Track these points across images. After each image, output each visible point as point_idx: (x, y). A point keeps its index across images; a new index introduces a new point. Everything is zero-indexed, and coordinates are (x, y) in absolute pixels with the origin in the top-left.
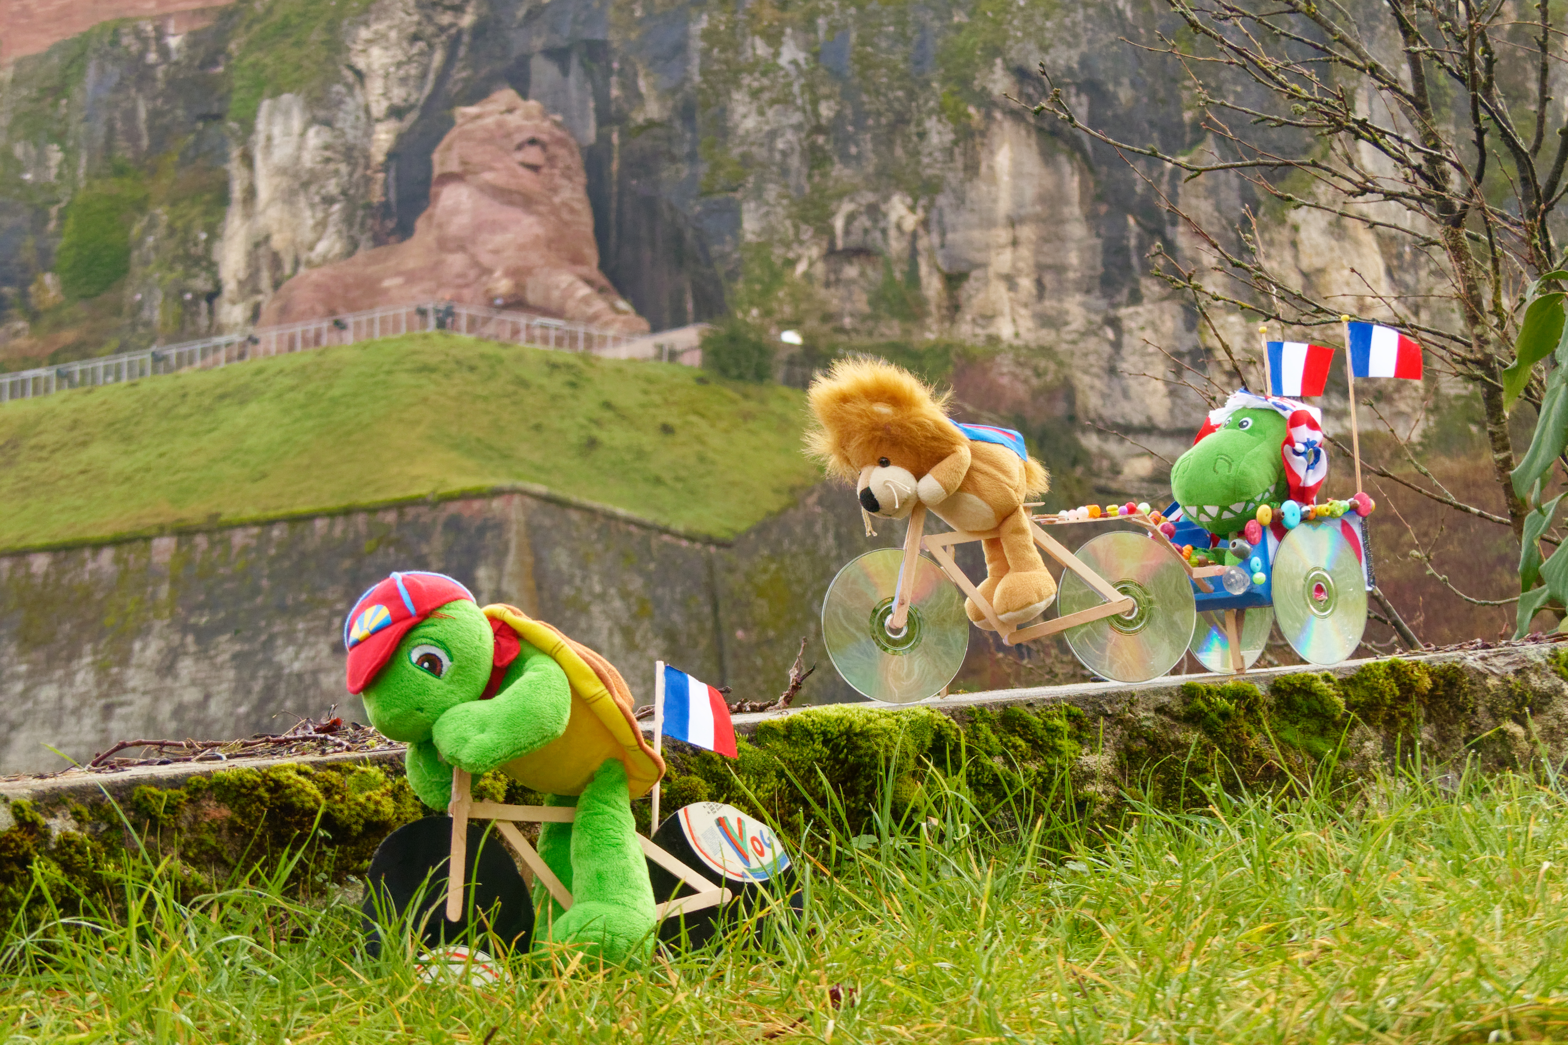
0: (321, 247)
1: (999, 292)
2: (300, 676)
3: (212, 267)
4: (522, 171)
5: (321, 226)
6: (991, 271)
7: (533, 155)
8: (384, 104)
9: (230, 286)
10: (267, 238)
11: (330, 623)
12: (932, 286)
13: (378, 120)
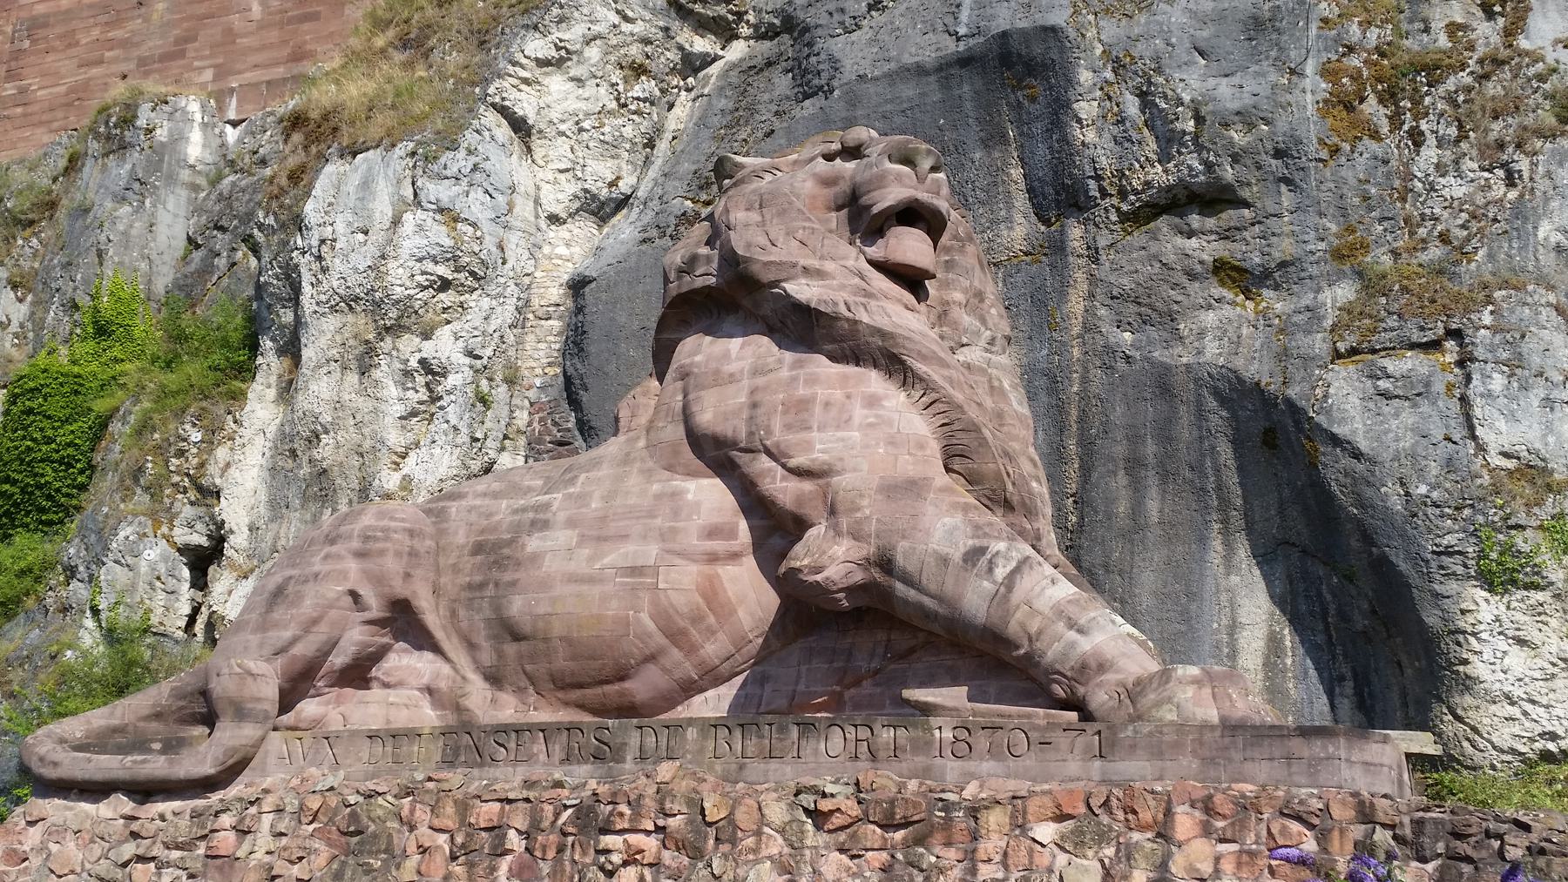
7: (910, 245)
8: (573, 188)
9: (238, 541)
13: (554, 219)
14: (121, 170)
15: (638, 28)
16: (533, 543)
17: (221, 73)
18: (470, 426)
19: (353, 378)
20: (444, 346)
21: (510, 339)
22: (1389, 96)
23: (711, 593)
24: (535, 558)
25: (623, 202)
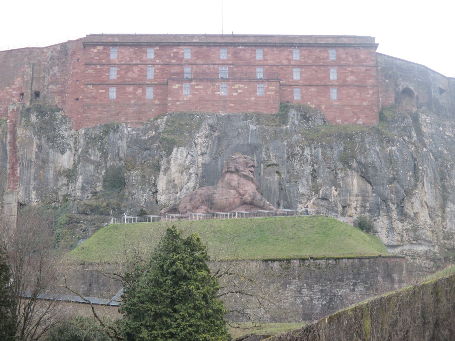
0: (188, 184)
1: (353, 211)
2: (341, 296)
3: (155, 186)
4: (250, 173)
5: (189, 179)
6: (352, 206)
8: (200, 152)
9: (160, 191)
10: (174, 181)
11: (350, 284)
12: (340, 208)
13: (199, 155)
14: (117, 135)
15: (208, 132)
16: (214, 195)
17: (126, 119)
19: (180, 174)
20: (191, 171)
22: (292, 157)
23: (234, 201)
24: (215, 197)
25: (206, 153)
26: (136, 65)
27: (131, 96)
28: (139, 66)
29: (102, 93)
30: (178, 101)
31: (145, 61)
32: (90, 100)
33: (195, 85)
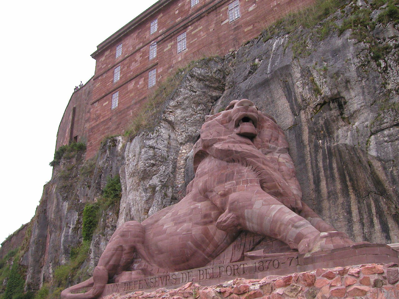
7: (247, 127)
13: (181, 144)
18: (161, 200)
20: (155, 180)
21: (172, 176)
26: (139, 50)
27: (133, 94)
28: (141, 50)
29: (105, 106)
30: (170, 67)
31: (148, 39)
32: (95, 121)
33: (192, 30)
